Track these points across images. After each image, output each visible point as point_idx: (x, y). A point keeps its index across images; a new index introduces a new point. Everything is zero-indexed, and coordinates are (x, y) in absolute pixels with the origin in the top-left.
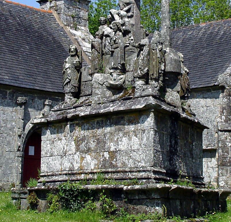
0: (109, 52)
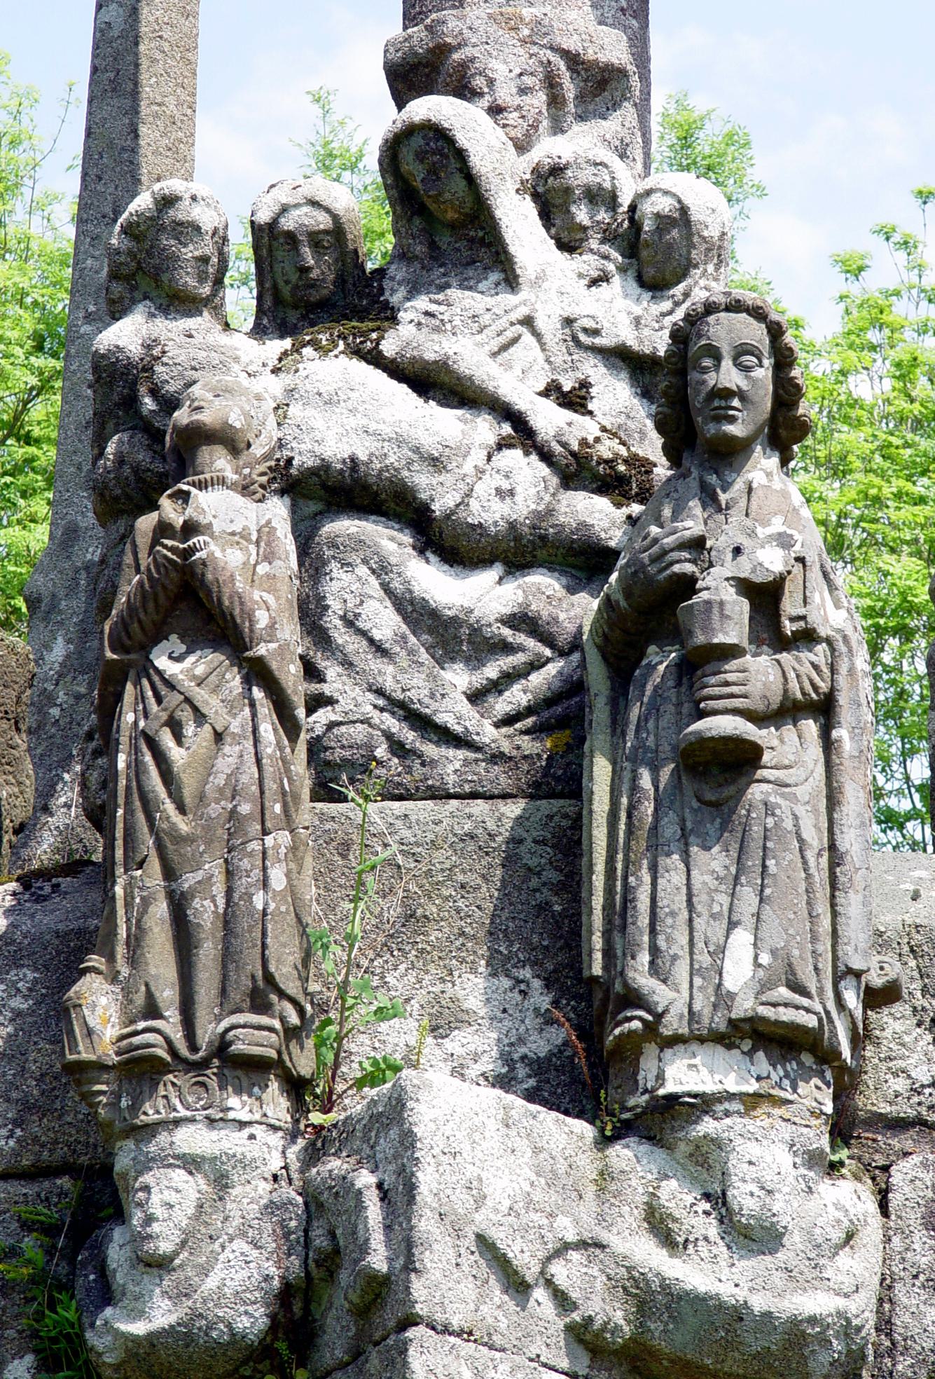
0: (398, 748)
